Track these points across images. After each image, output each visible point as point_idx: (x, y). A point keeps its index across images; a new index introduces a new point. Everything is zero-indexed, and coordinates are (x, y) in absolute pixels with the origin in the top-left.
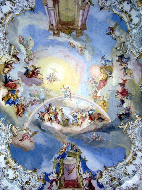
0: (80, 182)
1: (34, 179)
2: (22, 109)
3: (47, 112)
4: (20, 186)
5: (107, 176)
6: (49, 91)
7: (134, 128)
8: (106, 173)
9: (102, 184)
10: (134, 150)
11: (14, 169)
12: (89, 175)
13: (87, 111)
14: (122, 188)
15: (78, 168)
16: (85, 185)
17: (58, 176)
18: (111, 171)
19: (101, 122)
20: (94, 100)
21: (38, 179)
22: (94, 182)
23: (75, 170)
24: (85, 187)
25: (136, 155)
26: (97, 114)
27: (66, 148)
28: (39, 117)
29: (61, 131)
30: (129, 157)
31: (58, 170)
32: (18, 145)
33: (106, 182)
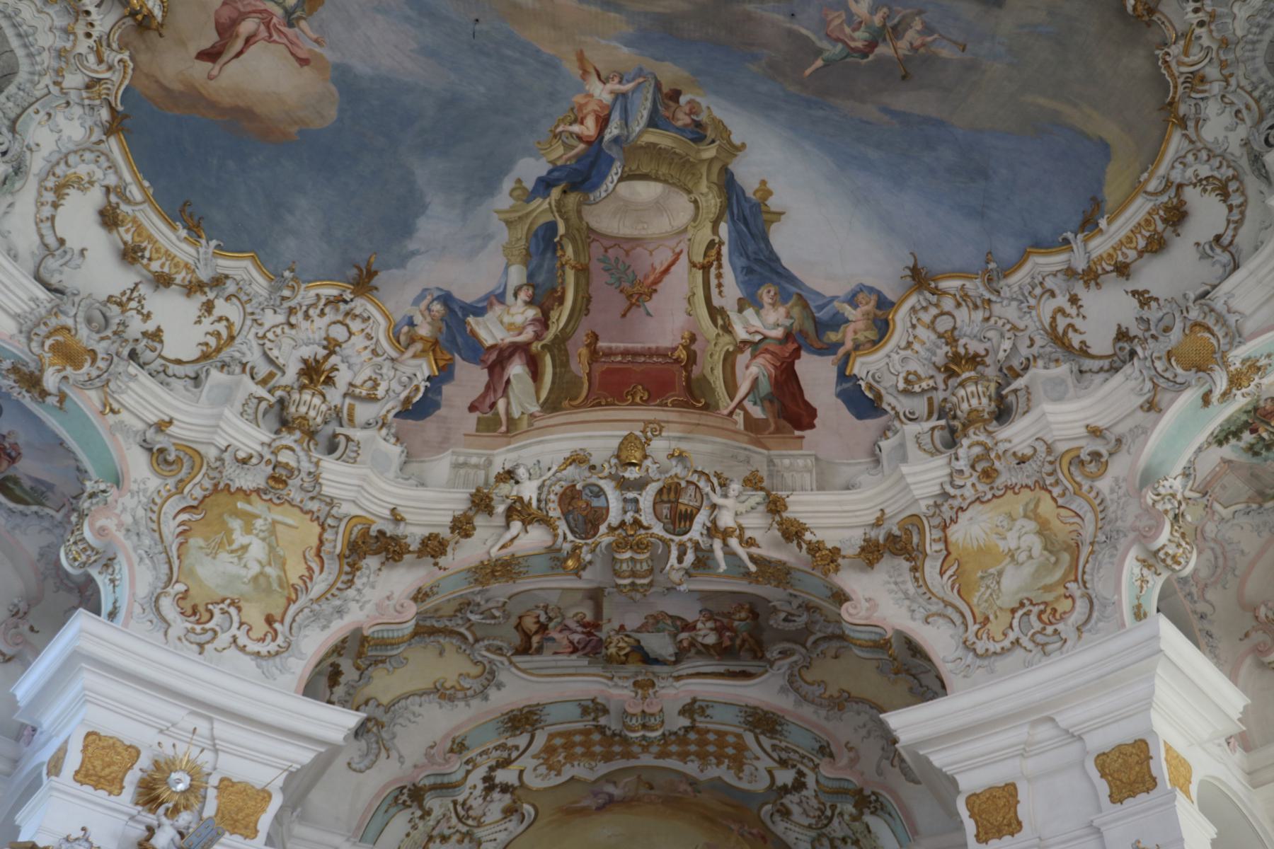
1: (359, 341)
5: (922, 332)
9: (871, 388)
10: (1176, 176)
11: (193, 288)
12: (788, 322)
14: (1007, 445)
15: (705, 268)
16: (744, 388)
17: (544, 322)
18: (959, 305)
21: (395, 338)
23: (681, 281)
24: (748, 404)
25: (1177, 215)
27: (611, 109)
31: (540, 279)
32: (193, 98)
33: (907, 381)
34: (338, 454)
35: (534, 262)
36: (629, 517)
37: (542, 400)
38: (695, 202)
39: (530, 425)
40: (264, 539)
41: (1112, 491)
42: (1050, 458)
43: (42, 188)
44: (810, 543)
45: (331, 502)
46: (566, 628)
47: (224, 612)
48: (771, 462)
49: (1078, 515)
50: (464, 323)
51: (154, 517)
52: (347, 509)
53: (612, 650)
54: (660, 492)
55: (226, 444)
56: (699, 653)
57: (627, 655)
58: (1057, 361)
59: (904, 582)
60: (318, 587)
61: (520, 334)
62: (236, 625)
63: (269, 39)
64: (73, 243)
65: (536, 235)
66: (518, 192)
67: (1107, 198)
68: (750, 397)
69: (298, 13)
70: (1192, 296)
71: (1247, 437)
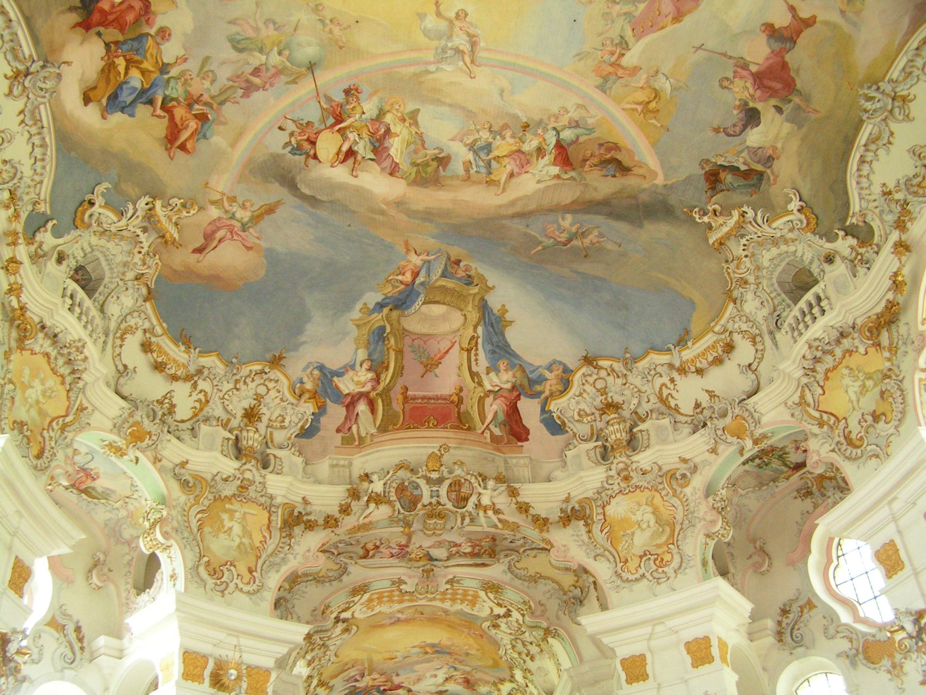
0: (471, 406)
1: (273, 393)
2: (196, 116)
3: (332, 126)
4: (231, 442)
5: (588, 388)
6: (349, 26)
7: (758, 243)
8: (589, 379)
9: (559, 418)
10: (730, 326)
11: (188, 378)
12: (514, 380)
13: (550, 127)
15: (469, 351)
16: (489, 418)
17: (377, 380)
18: (609, 375)
19: (614, 176)
20: (600, 81)
21: (293, 390)
22: (529, 410)
23: (455, 357)
24: (492, 427)
25: (730, 348)
26: (601, 145)
28: (287, 144)
29: (399, 204)
30: (697, 345)
32: (189, 273)
33: (579, 415)
34: (271, 469)
35: (372, 347)
36: (434, 500)
37: (377, 425)
38: (465, 315)
39: (372, 441)
40: (239, 523)
41: (692, 495)
42: (660, 474)
43: (115, 337)
44: (533, 516)
45: (272, 498)
46: (390, 547)
47: (229, 570)
48: (506, 461)
49: (674, 506)
50: (331, 381)
51: (186, 519)
52: (279, 500)
53: (413, 556)
54: (451, 485)
55: (216, 472)
56: (460, 556)
57: (420, 558)
58: (662, 414)
59: (582, 535)
60: (270, 549)
61: (363, 387)
62: (236, 577)
63: (232, 239)
64: (131, 367)
65: (373, 333)
66: (364, 310)
67: (692, 330)
68: (493, 422)
69: (249, 225)
70: (737, 401)
71: (757, 461)
